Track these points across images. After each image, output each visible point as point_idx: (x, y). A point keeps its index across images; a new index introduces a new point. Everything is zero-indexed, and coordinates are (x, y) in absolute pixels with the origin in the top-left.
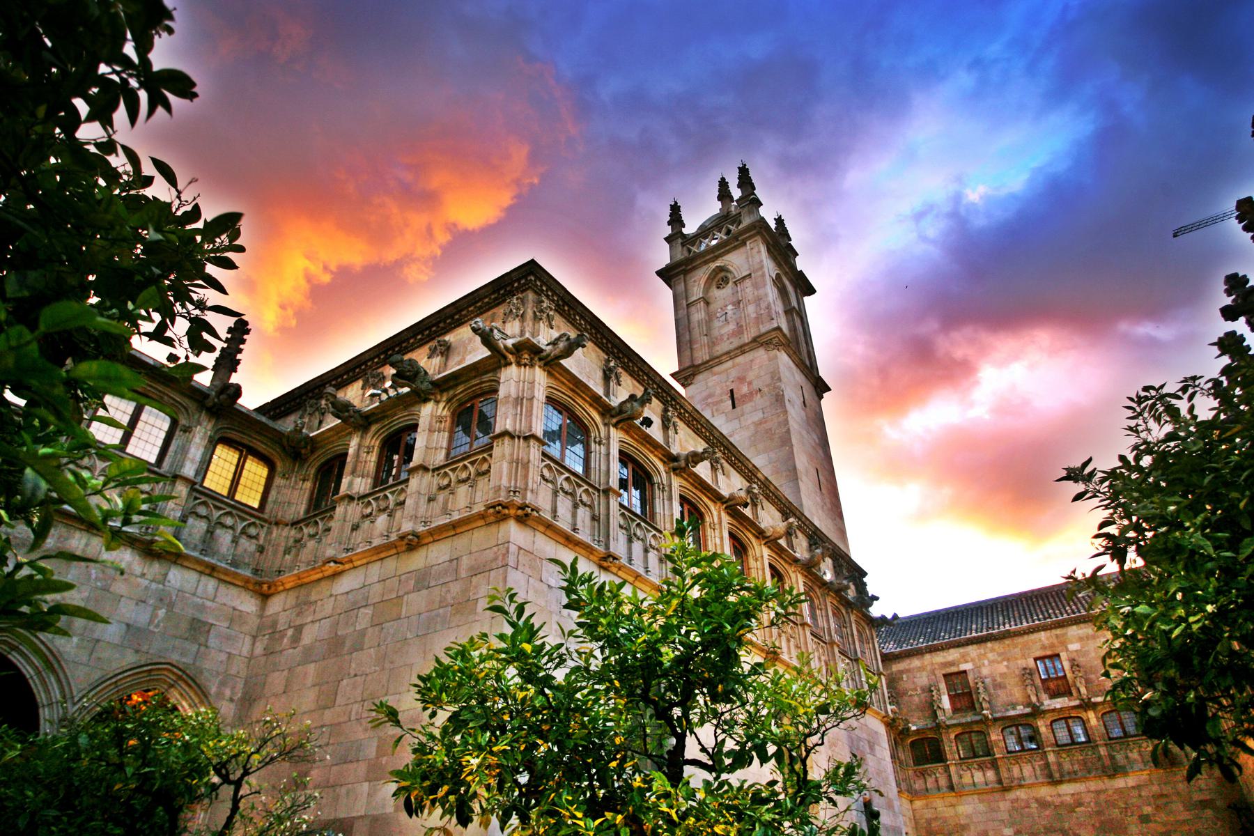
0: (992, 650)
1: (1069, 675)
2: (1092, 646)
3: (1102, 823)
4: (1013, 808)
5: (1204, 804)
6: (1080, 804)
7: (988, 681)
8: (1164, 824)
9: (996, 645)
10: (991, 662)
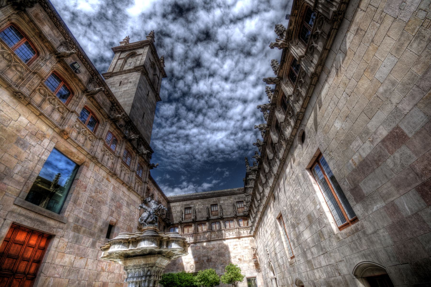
0: (200, 201)
2: (226, 202)
3: (219, 253)
4: (195, 249)
5: (246, 247)
6: (214, 248)
7: (197, 210)
8: (235, 254)
9: (201, 200)
10: (199, 205)
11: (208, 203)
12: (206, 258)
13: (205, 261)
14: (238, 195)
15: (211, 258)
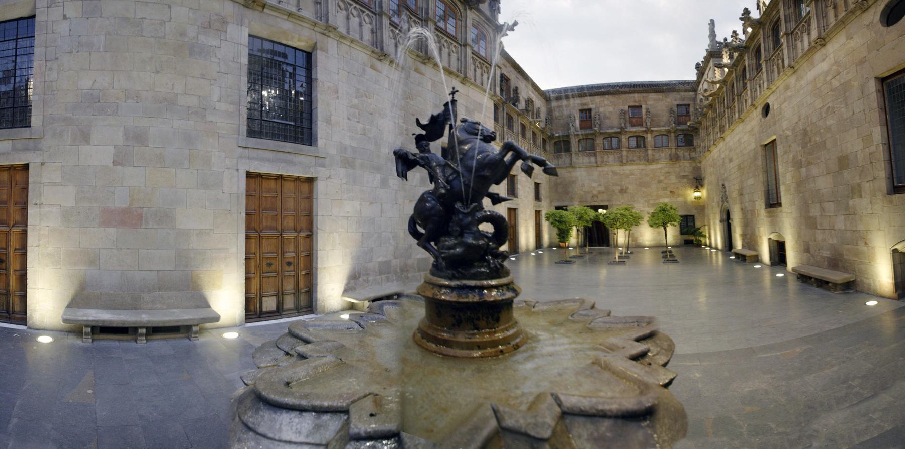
1: (644, 116)
5: (684, 177)
9: (610, 98)
11: (624, 103)
12: (619, 188)
13: (617, 191)
14: (682, 94)
15: (627, 188)
